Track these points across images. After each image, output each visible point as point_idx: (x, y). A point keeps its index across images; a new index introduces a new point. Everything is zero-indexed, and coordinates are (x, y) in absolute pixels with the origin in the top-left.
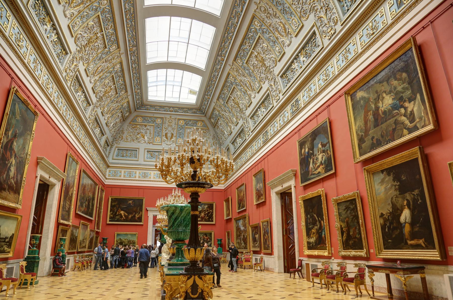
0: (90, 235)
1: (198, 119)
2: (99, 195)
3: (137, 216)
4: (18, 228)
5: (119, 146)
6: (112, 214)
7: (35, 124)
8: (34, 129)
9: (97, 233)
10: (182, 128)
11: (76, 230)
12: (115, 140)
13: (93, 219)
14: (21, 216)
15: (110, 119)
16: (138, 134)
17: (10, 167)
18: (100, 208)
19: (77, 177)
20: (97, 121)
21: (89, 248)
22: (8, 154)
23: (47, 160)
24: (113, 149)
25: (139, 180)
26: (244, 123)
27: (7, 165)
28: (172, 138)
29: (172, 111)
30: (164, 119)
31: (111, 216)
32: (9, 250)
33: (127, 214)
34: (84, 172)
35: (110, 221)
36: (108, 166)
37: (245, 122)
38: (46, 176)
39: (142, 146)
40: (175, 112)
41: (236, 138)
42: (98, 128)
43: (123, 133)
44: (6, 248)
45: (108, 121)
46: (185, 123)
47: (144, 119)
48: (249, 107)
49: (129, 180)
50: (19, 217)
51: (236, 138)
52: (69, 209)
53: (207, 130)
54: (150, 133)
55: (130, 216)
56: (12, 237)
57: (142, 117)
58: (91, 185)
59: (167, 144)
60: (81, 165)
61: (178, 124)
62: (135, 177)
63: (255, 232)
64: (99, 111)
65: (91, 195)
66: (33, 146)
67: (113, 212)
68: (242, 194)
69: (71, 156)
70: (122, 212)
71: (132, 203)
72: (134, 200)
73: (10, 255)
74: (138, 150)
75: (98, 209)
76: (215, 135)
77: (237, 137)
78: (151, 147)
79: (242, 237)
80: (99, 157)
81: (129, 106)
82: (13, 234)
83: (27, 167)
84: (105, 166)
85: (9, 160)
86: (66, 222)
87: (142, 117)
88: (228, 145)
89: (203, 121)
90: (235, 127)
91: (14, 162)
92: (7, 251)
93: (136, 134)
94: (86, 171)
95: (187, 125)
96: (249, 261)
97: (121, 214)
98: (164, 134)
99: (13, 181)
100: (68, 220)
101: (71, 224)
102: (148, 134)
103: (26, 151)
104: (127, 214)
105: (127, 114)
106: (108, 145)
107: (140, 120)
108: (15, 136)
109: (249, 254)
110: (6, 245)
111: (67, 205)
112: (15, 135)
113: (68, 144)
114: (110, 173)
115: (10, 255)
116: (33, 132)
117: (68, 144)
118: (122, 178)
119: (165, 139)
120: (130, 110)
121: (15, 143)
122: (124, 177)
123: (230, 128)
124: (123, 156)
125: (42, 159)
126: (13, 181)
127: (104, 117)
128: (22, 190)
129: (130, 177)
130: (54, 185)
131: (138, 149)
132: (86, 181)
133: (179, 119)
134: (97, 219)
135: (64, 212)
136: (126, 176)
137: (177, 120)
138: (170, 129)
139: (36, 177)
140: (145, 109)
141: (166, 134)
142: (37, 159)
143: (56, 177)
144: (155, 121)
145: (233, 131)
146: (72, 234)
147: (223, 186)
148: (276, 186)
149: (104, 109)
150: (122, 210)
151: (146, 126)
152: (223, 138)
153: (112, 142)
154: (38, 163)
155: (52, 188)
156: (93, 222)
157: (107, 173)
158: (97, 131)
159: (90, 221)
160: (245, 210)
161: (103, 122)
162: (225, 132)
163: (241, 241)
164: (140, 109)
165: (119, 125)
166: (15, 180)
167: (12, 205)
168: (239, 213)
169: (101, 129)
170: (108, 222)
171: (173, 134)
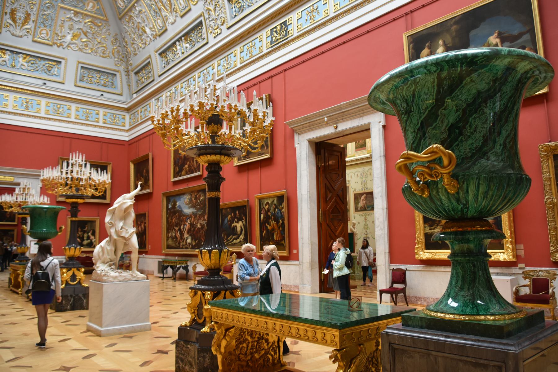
26: (209, 10)
37: (211, 8)
41: (174, 43)
53: (103, 22)
59: (13, 35)
63: (235, 216)
76: (119, 37)
77: (179, 40)
79: (187, 226)
88: (149, 57)
90: (178, 19)
98: (8, 11)
119: (12, 23)
123: (164, 23)
141: (13, 13)
145: (169, 27)
147: (127, 134)
148: (312, 126)
152: (138, 41)
162: (148, 30)
163: (182, 235)
168: (175, 183)
171: (29, 15)
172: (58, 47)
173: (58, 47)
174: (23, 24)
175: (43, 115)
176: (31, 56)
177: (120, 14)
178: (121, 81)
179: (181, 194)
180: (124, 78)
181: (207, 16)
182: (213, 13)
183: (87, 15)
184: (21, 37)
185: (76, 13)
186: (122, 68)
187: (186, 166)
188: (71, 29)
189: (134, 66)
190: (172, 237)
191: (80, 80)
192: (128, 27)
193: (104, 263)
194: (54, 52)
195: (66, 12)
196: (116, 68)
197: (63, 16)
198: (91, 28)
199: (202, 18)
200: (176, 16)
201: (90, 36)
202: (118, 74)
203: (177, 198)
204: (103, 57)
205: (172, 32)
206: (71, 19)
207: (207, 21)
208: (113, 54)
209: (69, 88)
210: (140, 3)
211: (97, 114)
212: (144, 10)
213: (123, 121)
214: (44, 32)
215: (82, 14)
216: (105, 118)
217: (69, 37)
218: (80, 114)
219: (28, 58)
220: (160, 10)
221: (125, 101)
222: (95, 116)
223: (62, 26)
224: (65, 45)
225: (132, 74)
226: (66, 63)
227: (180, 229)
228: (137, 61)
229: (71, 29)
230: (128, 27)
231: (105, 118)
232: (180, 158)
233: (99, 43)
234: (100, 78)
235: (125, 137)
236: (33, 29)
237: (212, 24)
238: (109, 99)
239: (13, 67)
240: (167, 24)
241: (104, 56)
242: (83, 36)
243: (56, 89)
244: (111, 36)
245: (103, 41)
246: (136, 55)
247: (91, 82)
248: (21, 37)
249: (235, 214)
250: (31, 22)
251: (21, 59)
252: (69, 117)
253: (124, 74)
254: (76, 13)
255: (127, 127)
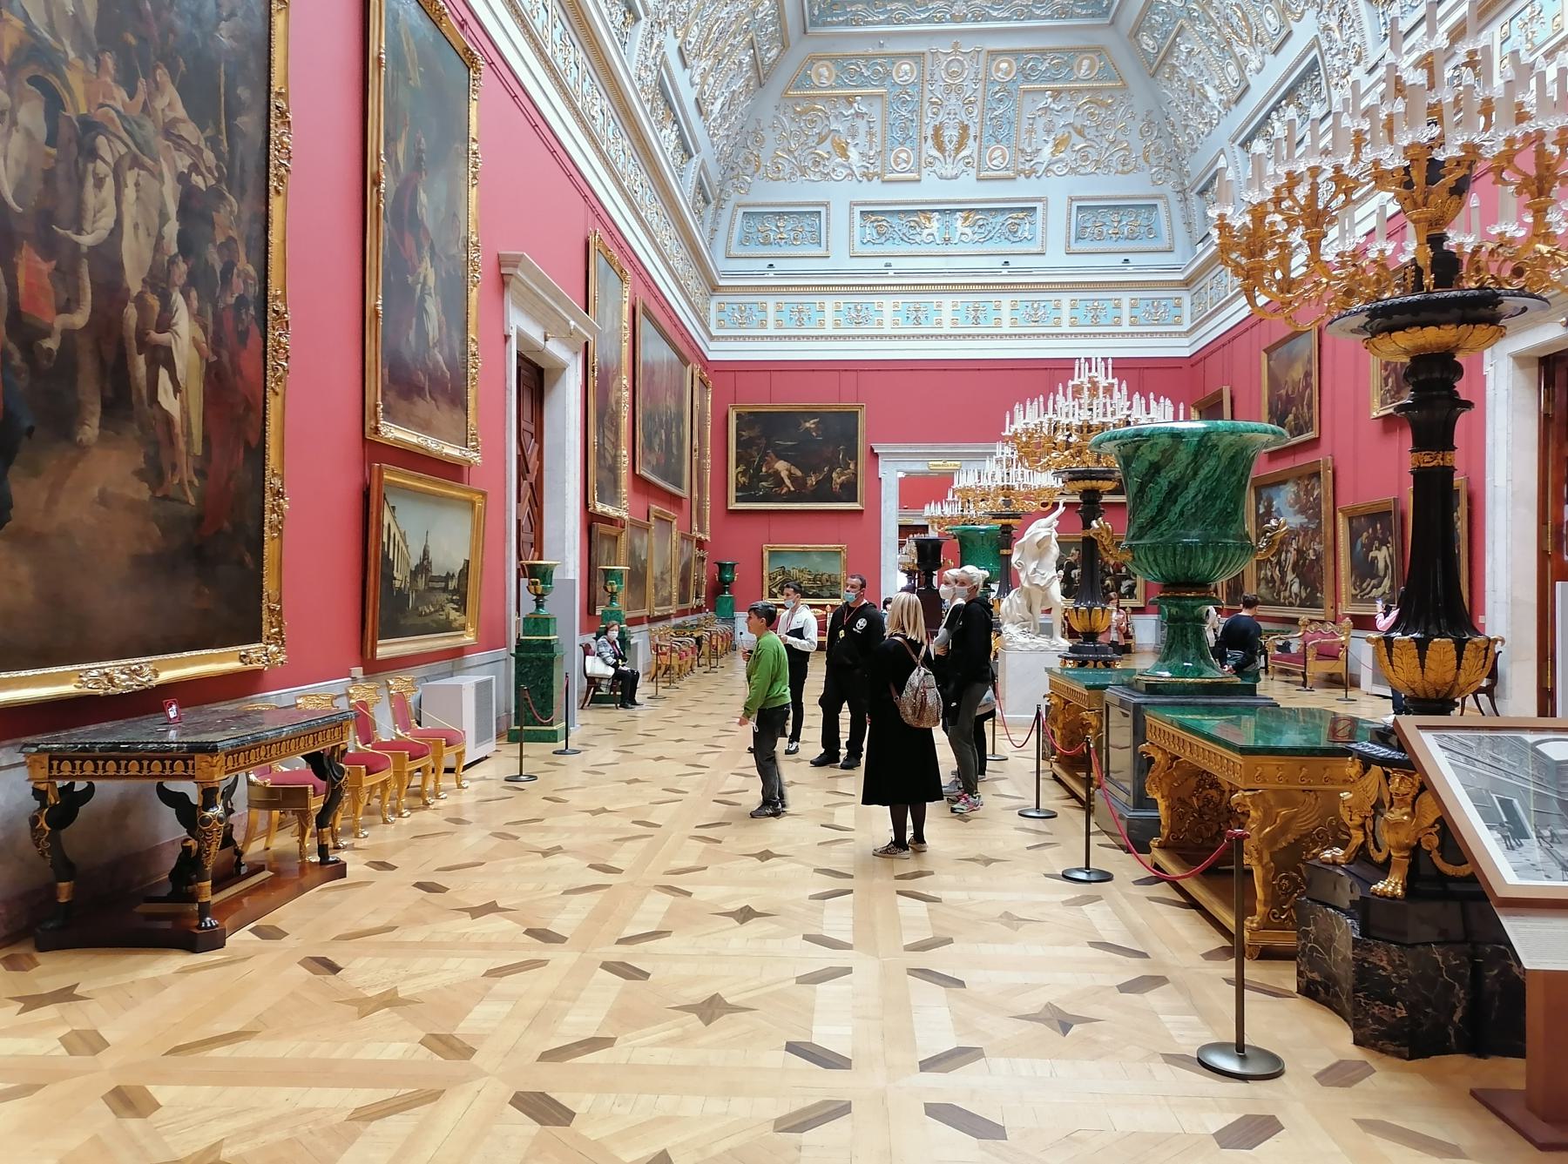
0: (681, 551)
1: (1081, 43)
2: (696, 402)
3: (838, 478)
4: (482, 536)
5: (746, 200)
6: (744, 473)
7: (474, 105)
8: (473, 134)
9: (701, 544)
10: (1007, 93)
11: (642, 539)
12: (730, 174)
13: (685, 493)
14: (484, 494)
15: (711, 80)
16: (822, 140)
17: (422, 300)
18: (702, 455)
19: (628, 334)
20: (664, 92)
21: (681, 602)
22: (409, 242)
23: (534, 269)
24: (726, 215)
25: (835, 337)
26: (1327, 28)
27: (412, 290)
28: (961, 145)
29: (964, 19)
30: (929, 58)
31: (742, 480)
32: (461, 619)
33: (799, 473)
34: (647, 313)
35: (738, 500)
36: (715, 289)
37: (1333, 24)
38: (535, 333)
39: (841, 194)
40: (976, 21)
41: (1268, 116)
42: (669, 125)
43: (759, 142)
44: (454, 615)
45: (702, 93)
46: (1021, 71)
47: (845, 70)
49: (798, 338)
50: (477, 498)
51: (1268, 116)
52: (615, 457)
53: (1117, 94)
54: (870, 134)
55: (812, 481)
56: (464, 573)
57: (830, 58)
58: (670, 363)
60: (633, 287)
61: (988, 81)
62: (822, 324)
63: (1371, 540)
64: (671, 46)
65: (671, 402)
66: (480, 206)
67: (749, 464)
68: (1297, 373)
69: (599, 251)
70: (781, 466)
71: (817, 429)
72: (822, 416)
73: (469, 638)
74: (822, 210)
75: (696, 454)
78: (876, 193)
79: (1292, 556)
80: (683, 252)
81: (780, 16)
82: (467, 562)
83: (473, 295)
84: (702, 289)
85: (414, 271)
86: (609, 510)
87: (830, 58)
89: (1098, 50)
90: (1269, 58)
91: (431, 281)
92: (456, 625)
93: (812, 142)
94: (649, 311)
95: (1027, 78)
96: (1336, 658)
97: (777, 473)
98: (930, 132)
99: (440, 358)
100: (613, 499)
101: (625, 515)
102: (862, 138)
103: (463, 234)
104: (799, 473)
105: (774, 52)
106: (707, 201)
107: (824, 73)
108: (417, 164)
109: (1329, 627)
110: (452, 601)
111: (608, 446)
112: (420, 159)
113: (585, 197)
114: (722, 316)
115: (469, 638)
116: (474, 146)
117: (585, 197)
118: (771, 331)
120: (783, 30)
121: (423, 197)
122: (779, 327)
123: (1241, 70)
124: (766, 242)
125: (516, 262)
126: (440, 358)
127: (688, 71)
128: (471, 393)
129: (801, 325)
130: (561, 369)
131: (826, 205)
132: (655, 351)
133: (994, 54)
134: (695, 495)
135: (599, 474)
136: (786, 322)
137: (982, 57)
138: (953, 102)
139: (507, 338)
140: (846, 23)
142: (500, 262)
143: (568, 336)
144: (888, 74)
145: (1253, 80)
146: (632, 555)
147: (1186, 341)
149: (686, 35)
150: (780, 457)
151: (849, 100)
152: (1195, 121)
153: (721, 183)
154: (503, 282)
155: (556, 381)
156: (686, 504)
157: (713, 316)
158: (669, 135)
159: (675, 501)
160: (1314, 443)
161: (688, 96)
162: (1211, 93)
164: (825, 24)
165: (744, 103)
166: (446, 350)
167: (452, 451)
169: (680, 129)
170: (734, 505)
171: (965, 128)
172: (1028, 177)
173: (1028, 177)
174: (958, 150)
175: (1006, 330)
176: (977, 210)
177: (1151, 65)
178: (1169, 217)
179: (1278, 482)
180: (1176, 208)
181: (1325, 45)
182: (1337, 35)
183: (1079, 90)
184: (956, 177)
185: (1057, 94)
186: (1168, 189)
187: (1291, 417)
188: (1049, 132)
189: (1194, 176)
190: (1265, 578)
191: (1078, 238)
192: (1171, 92)
193: (1013, 623)
194: (1022, 189)
195: (1037, 97)
196: (1154, 191)
197: (1030, 107)
198: (1092, 114)
199: (1316, 51)
200: (1264, 53)
201: (1091, 133)
203: (1273, 492)
204: (1123, 173)
205: (1262, 87)
206: (1046, 109)
207: (1328, 58)
209: (1056, 260)
210: (1187, 34)
211: (1117, 307)
212: (1196, 50)
213: (1176, 311)
214: (998, 153)
215: (1069, 90)
216: (1135, 312)
217: (1047, 150)
218: (1080, 313)
219: (973, 217)
220: (1229, 44)
221: (1183, 260)
222: (1112, 313)
223: (1031, 131)
224: (1041, 169)
225: (1193, 196)
226: (1046, 209)
227: (1279, 563)
228: (1196, 166)
229: (1049, 132)
230: (1171, 92)
231: (1135, 312)
232: (1280, 397)
235: (1181, 348)
236: (975, 155)
237: (1338, 64)
238: (1146, 265)
239: (947, 241)
240: (1248, 74)
241: (1126, 168)
242: (1075, 137)
243: (1028, 271)
244: (1138, 118)
245: (1120, 137)
247: (1100, 237)
248: (956, 177)
249: (1375, 530)
250: (971, 141)
251: (959, 222)
252: (1058, 325)
253: (1174, 199)
254: (1057, 94)
255: (1187, 326)
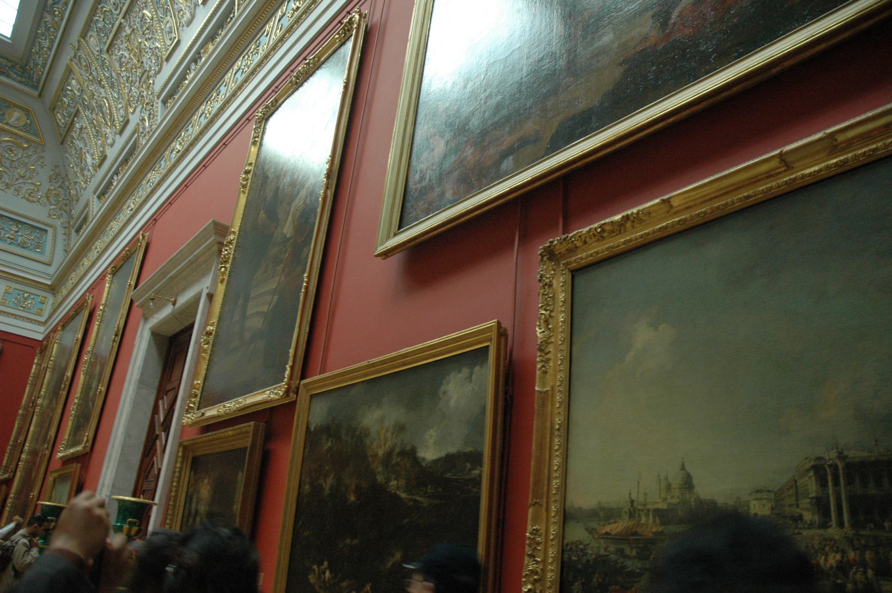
48: (168, 59)
89: (27, 112)
90: (118, 136)
180: (60, 238)
186: (58, 223)
196: (49, 221)
202: (50, 230)
204: (28, 200)
208: (48, 197)
233: (22, 177)
234: (16, 232)
241: (30, 198)
245: (28, 174)
246: (77, 200)
253: (60, 231)
